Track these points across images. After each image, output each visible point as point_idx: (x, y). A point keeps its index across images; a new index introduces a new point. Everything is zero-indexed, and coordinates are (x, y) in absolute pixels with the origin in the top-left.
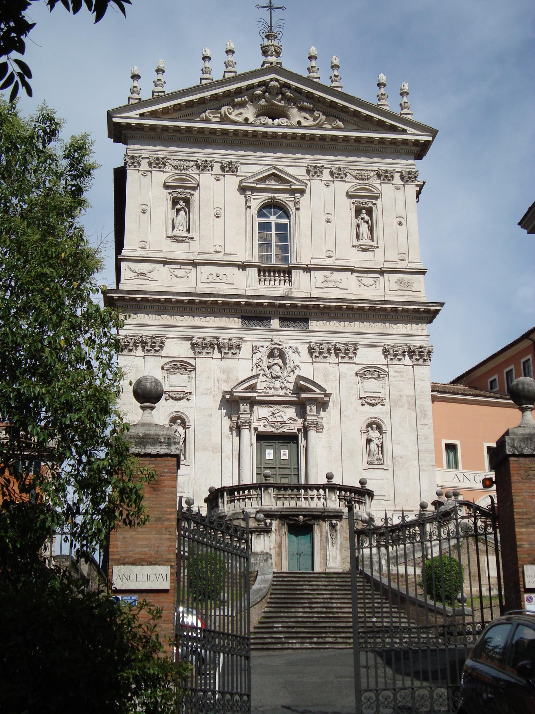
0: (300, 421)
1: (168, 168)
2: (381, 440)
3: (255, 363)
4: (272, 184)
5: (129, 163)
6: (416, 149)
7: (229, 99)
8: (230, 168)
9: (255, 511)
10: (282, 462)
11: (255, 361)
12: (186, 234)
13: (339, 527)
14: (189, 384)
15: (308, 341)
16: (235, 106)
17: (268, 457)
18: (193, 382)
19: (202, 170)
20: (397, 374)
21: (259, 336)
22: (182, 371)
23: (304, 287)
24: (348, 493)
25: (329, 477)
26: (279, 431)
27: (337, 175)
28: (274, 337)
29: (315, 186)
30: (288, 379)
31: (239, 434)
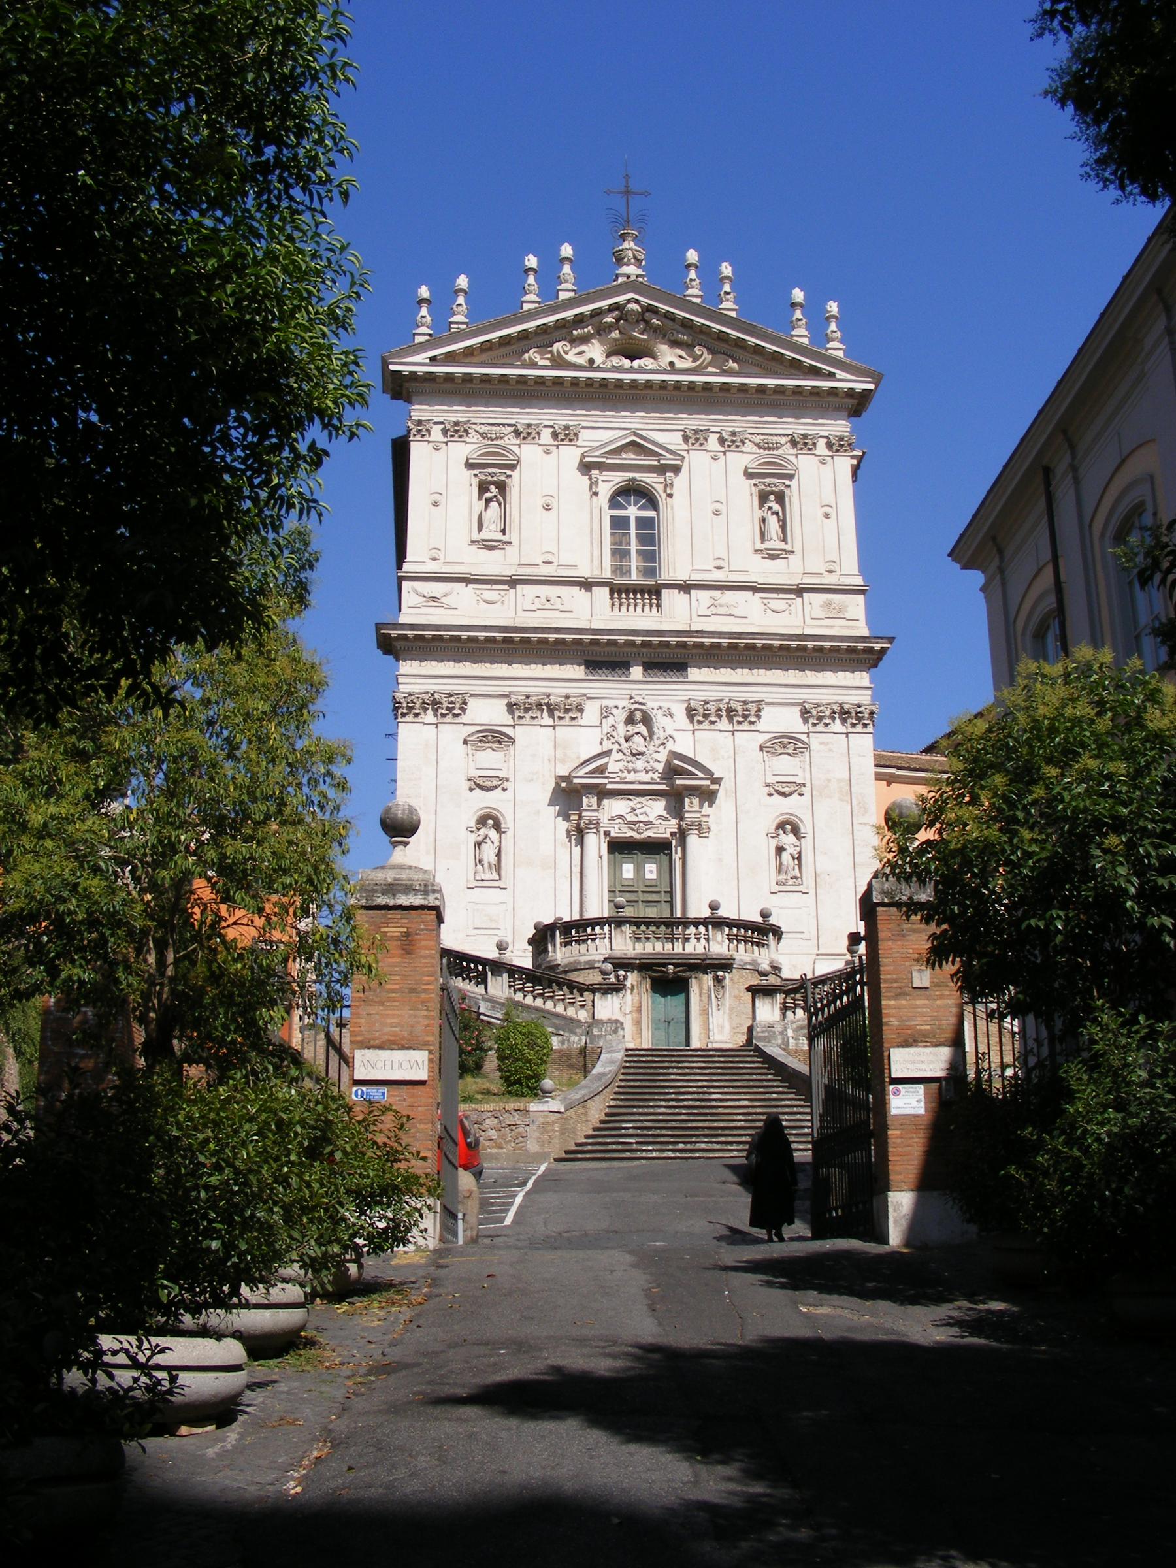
0: (674, 822)
1: (474, 437)
2: (798, 849)
4: (629, 458)
5: (413, 432)
6: (850, 402)
7: (564, 331)
8: (566, 435)
9: (601, 958)
10: (648, 883)
11: (606, 729)
12: (500, 536)
13: (727, 982)
16: (574, 341)
17: (625, 875)
18: (512, 762)
19: (524, 438)
22: (494, 746)
23: (678, 615)
24: (743, 931)
25: (714, 907)
26: (643, 836)
27: (730, 443)
28: (634, 693)
29: (697, 462)
30: (656, 756)
31: (581, 842)
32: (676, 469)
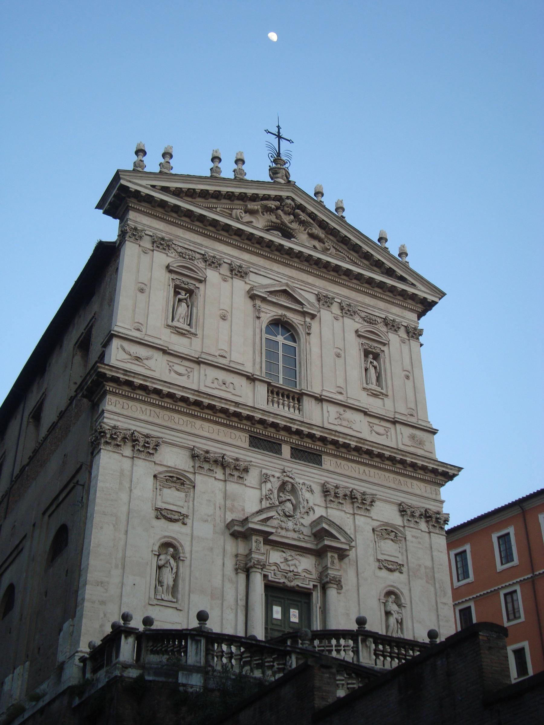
3: (264, 493)
5: (129, 234)
12: (188, 328)
14: (186, 504)
15: (323, 482)
18: (191, 503)
20: (414, 539)
21: (269, 464)
30: (302, 521)
32: (313, 317)
